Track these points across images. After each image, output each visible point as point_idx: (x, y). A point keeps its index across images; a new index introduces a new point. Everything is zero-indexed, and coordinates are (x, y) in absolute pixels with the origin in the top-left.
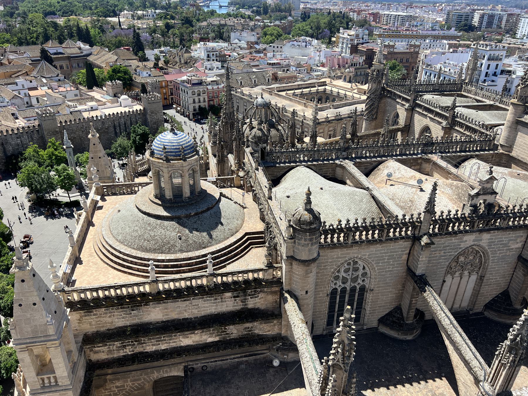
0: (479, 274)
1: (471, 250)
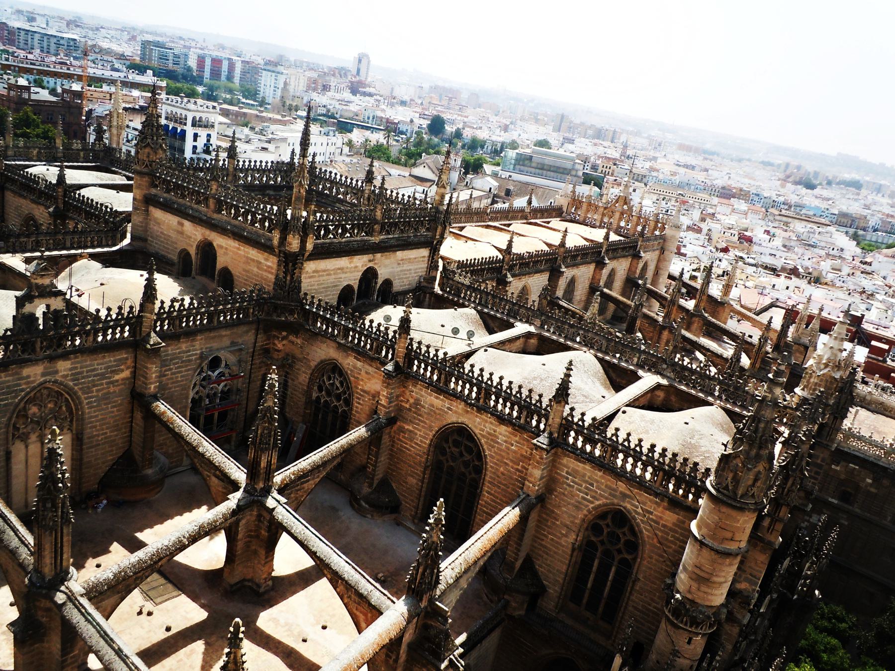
0: (74, 432)
1: (45, 392)
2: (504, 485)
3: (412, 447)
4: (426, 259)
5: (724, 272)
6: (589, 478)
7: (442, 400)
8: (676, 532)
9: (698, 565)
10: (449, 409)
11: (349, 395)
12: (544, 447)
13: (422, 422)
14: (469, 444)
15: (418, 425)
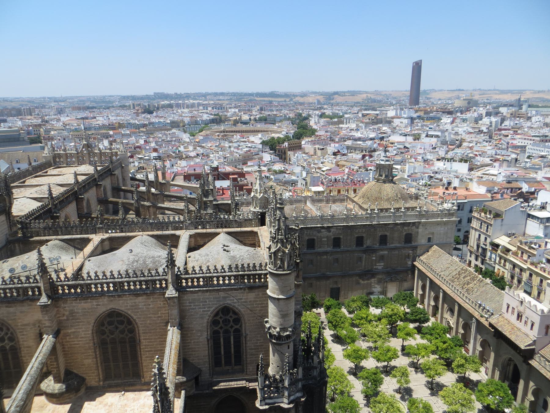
2: (152, 330)
3: (80, 341)
4: (5, 222)
5: (139, 168)
6: (203, 299)
7: (90, 302)
8: (257, 301)
9: (280, 310)
10: (97, 305)
11: (12, 333)
12: (174, 295)
13: (81, 322)
14: (119, 319)
15: (78, 325)
